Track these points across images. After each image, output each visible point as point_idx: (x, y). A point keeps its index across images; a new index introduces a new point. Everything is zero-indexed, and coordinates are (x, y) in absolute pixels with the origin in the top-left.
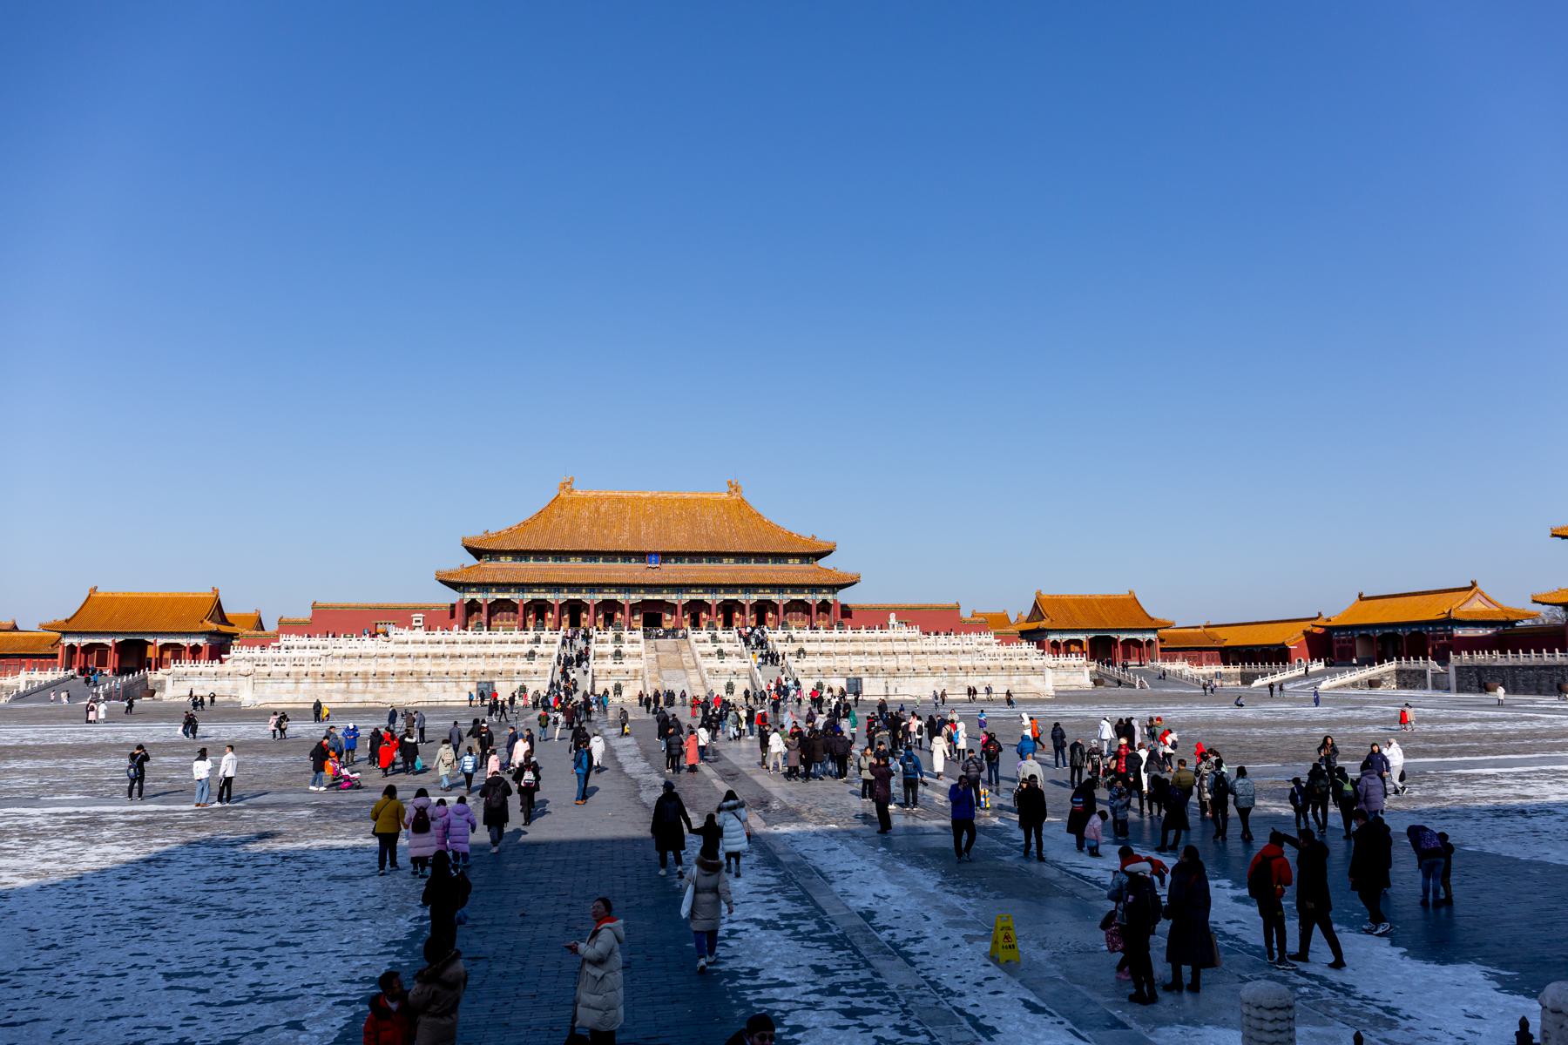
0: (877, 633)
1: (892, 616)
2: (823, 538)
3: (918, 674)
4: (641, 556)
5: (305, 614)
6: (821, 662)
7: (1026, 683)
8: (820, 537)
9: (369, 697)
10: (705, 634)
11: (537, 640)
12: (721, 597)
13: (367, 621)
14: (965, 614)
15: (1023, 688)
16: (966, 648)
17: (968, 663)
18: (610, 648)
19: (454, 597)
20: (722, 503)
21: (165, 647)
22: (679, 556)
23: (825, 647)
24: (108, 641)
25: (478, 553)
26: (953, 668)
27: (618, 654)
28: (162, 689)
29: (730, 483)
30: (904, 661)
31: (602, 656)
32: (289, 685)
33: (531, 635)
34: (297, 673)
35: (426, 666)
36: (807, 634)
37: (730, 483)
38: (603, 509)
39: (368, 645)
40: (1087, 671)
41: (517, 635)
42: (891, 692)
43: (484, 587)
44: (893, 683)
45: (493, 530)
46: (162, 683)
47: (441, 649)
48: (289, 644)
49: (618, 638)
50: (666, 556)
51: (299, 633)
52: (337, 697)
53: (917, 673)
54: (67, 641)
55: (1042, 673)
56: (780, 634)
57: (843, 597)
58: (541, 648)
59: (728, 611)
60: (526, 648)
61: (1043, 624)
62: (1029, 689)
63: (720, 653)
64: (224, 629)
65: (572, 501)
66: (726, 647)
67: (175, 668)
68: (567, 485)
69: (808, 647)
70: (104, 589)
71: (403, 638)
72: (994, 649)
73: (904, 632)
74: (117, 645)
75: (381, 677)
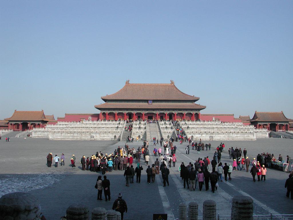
0: (209, 122)
2: (197, 96)
3: (219, 134)
4: (147, 101)
5: (64, 116)
6: (193, 130)
7: (248, 136)
8: (195, 96)
9: (78, 138)
10: (163, 122)
11: (119, 124)
12: (168, 112)
13: (78, 118)
14: (235, 117)
15: (248, 138)
16: (233, 127)
17: (233, 131)
18: (138, 126)
19: (99, 112)
20: (169, 86)
21: (32, 124)
23: (194, 126)
24: (19, 123)
25: (105, 100)
27: (140, 128)
28: (32, 135)
29: (171, 81)
31: (136, 128)
32: (60, 134)
33: (118, 122)
34: (61, 132)
35: (92, 130)
36: (190, 122)
37: (171, 81)
39: (78, 124)
40: (267, 133)
41: (114, 122)
46: (32, 133)
47: (95, 126)
48: (60, 124)
49: (140, 123)
50: (154, 101)
51: (62, 121)
52: (71, 138)
54: (10, 123)
56: (183, 122)
57: (202, 112)
58: (120, 126)
59: (171, 117)
60: (117, 126)
61: (256, 120)
62: (250, 138)
63: (166, 127)
64: (45, 120)
66: (168, 126)
67: (34, 129)
68: (127, 83)
69: (190, 126)
71: (86, 123)
72: (242, 126)
73: (217, 123)
74: (21, 124)
75: (81, 133)
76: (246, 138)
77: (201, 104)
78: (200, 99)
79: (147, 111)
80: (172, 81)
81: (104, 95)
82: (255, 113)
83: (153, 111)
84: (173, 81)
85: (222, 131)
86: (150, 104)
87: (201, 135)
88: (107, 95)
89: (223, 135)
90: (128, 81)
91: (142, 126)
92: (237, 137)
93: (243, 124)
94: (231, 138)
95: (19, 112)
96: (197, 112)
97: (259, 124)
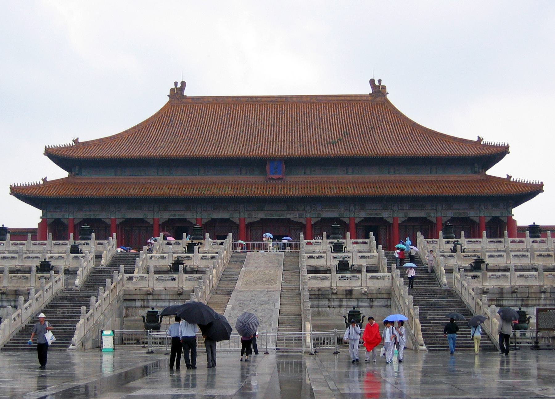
2: (492, 138)
8: (488, 139)
27: (175, 267)
29: (372, 82)
37: (372, 82)
63: (343, 267)
68: (177, 93)
77: (516, 177)
78: (510, 150)
79: (261, 209)
80: (377, 83)
81: (63, 140)
83: (290, 208)
84: (380, 81)
86: (276, 176)
88: (76, 141)
90: (179, 86)
91: (195, 260)
96: (496, 214)
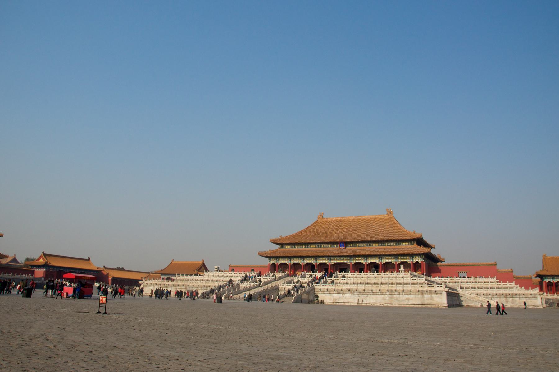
1: (402, 267)
7: (431, 299)
19: (266, 262)
20: (383, 219)
22: (354, 243)
26: (391, 290)
29: (387, 210)
30: (368, 287)
37: (387, 210)
38: (332, 225)
42: (361, 301)
43: (277, 258)
44: (362, 297)
45: (284, 235)
53: (373, 292)
55: (441, 294)
62: (434, 302)
65: (322, 222)
70: (175, 261)
76: (426, 302)
82: (541, 258)
85: (381, 289)
87: (343, 294)
88: (281, 237)
89: (383, 296)
92: (408, 299)
93: (498, 281)
94: (396, 302)
95: (176, 264)
97: (547, 280)
